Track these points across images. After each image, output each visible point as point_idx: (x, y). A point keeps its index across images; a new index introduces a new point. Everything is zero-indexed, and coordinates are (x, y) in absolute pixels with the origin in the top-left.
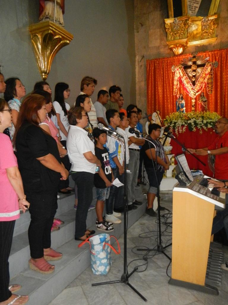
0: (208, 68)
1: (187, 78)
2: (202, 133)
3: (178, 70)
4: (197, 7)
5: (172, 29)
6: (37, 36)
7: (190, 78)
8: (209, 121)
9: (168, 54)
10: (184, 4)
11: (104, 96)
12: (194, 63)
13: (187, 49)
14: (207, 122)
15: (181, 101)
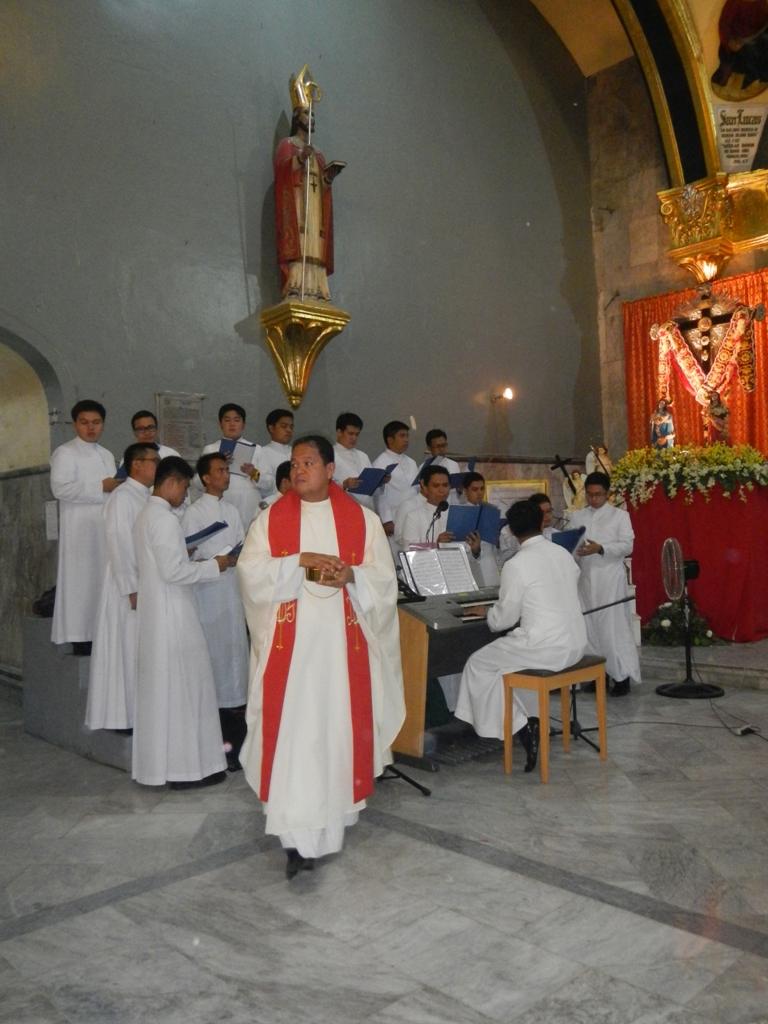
0: (738, 324)
1: (688, 353)
2: (691, 500)
3: (663, 334)
4: (752, 145)
5: (680, 215)
6: (276, 331)
7: (696, 354)
8: (716, 469)
9: (683, 280)
10: (707, 140)
11: (394, 438)
12: (706, 313)
13: (731, 261)
14: (710, 474)
15: (660, 419)
